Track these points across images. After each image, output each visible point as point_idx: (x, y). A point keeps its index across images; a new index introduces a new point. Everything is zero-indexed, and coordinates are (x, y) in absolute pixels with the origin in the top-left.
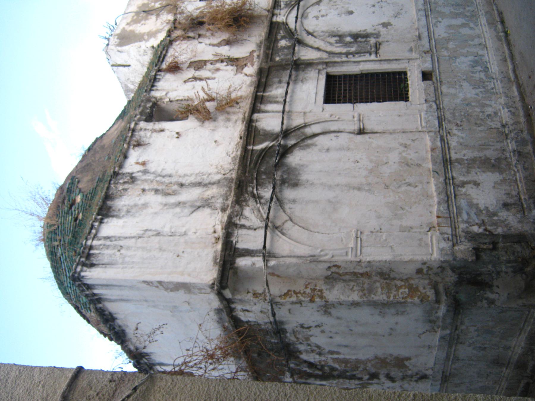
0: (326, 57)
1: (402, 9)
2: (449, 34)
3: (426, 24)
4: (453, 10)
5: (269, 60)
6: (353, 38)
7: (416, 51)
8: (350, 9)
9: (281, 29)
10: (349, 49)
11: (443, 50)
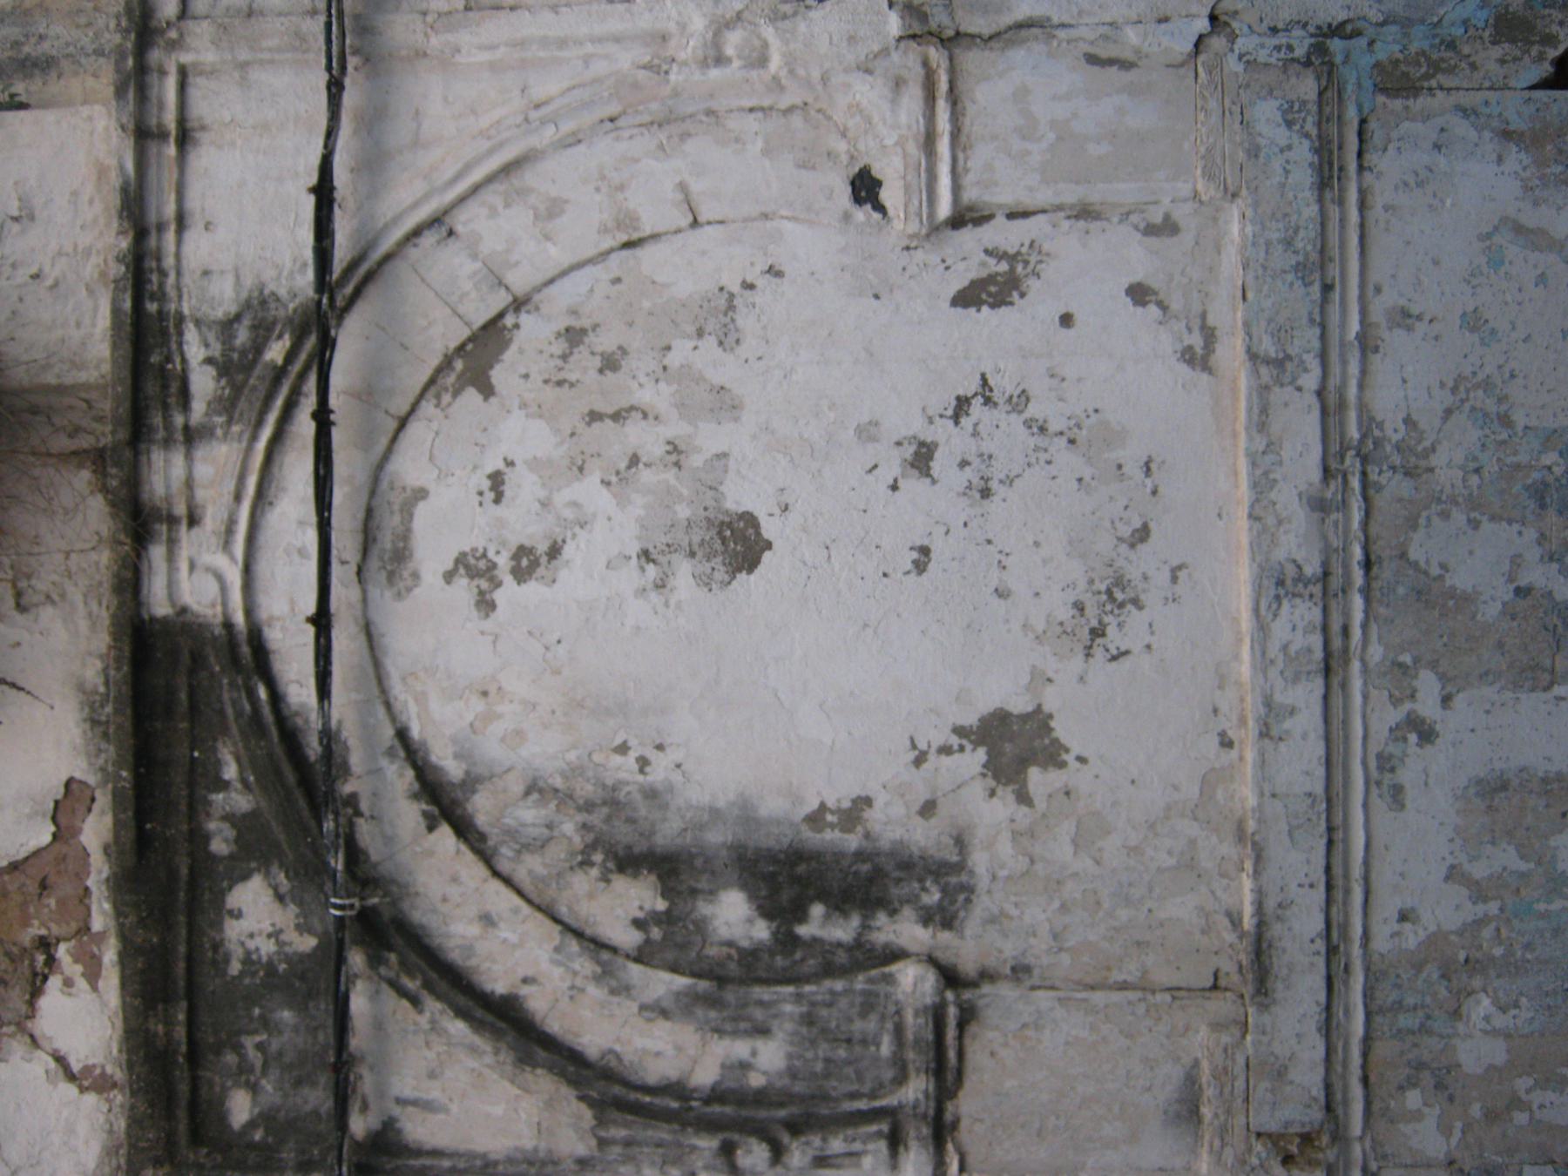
0: (582, 1149)
1: (1143, 534)
2: (1479, 892)
3: (1319, 789)
4: (1537, 575)
5: (182, 1127)
6: (767, 912)
7: (1223, 1131)
8: (739, 496)
9: (225, 730)
10: (740, 1048)
11: (1413, 1099)
